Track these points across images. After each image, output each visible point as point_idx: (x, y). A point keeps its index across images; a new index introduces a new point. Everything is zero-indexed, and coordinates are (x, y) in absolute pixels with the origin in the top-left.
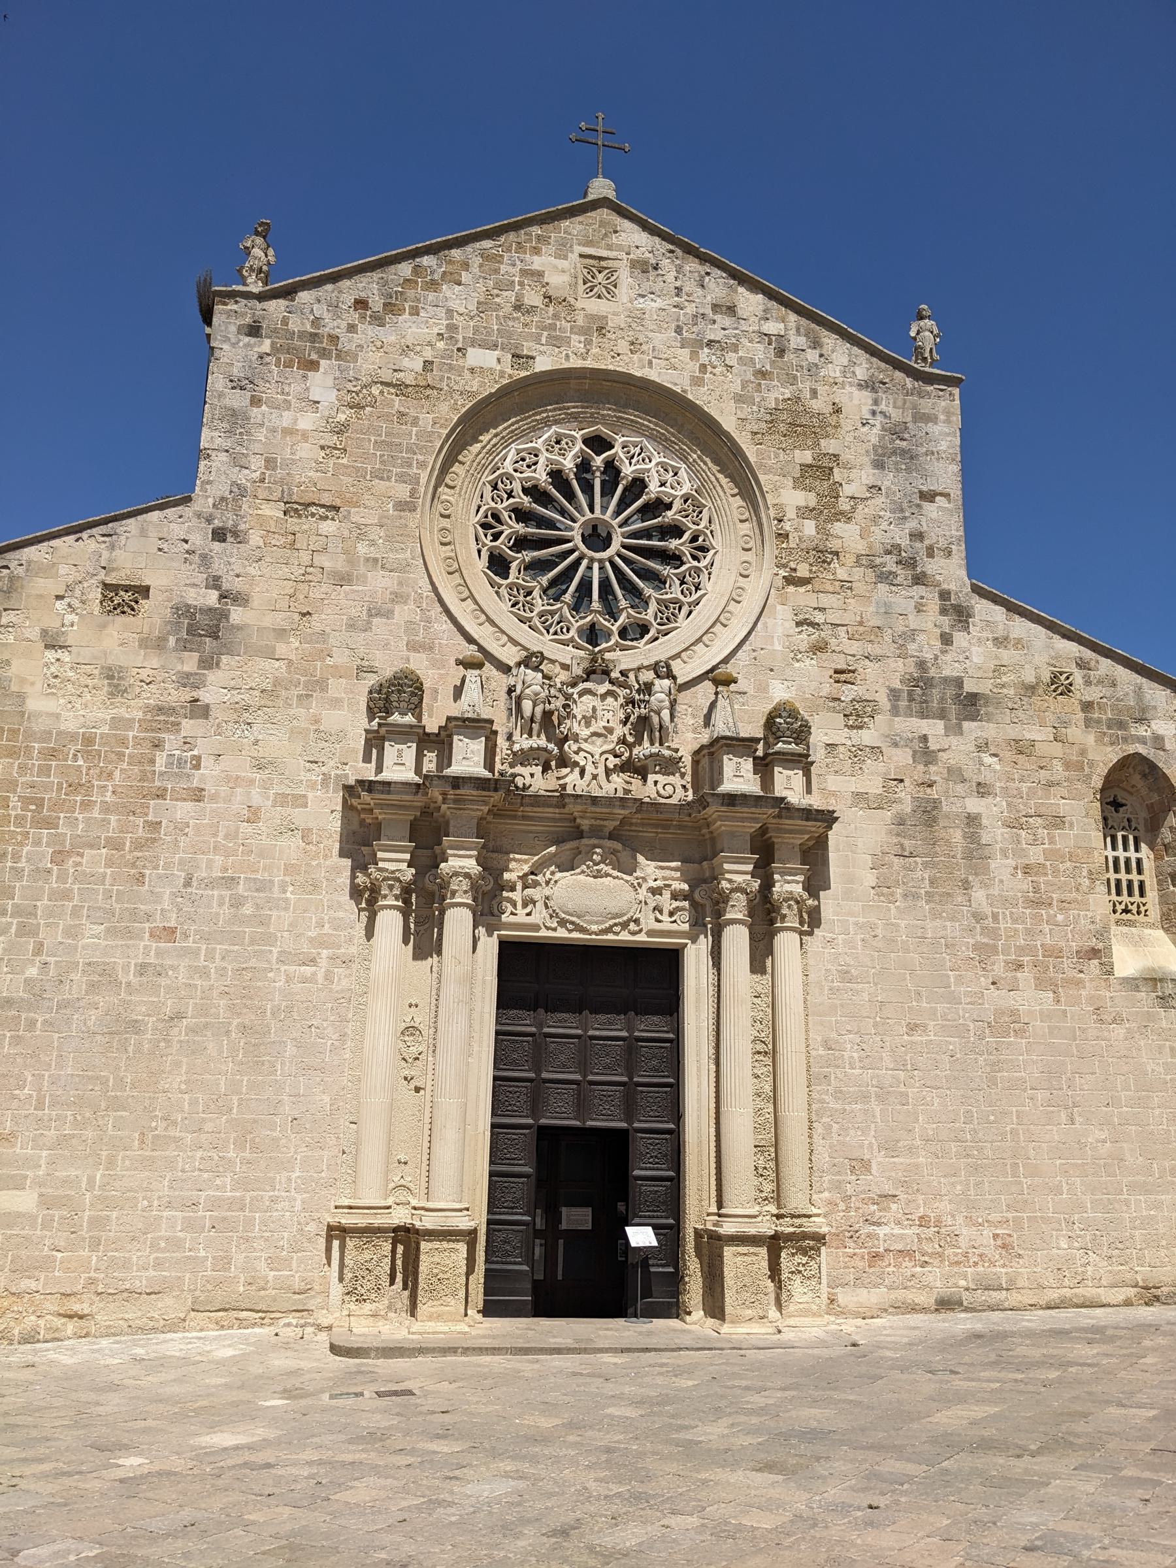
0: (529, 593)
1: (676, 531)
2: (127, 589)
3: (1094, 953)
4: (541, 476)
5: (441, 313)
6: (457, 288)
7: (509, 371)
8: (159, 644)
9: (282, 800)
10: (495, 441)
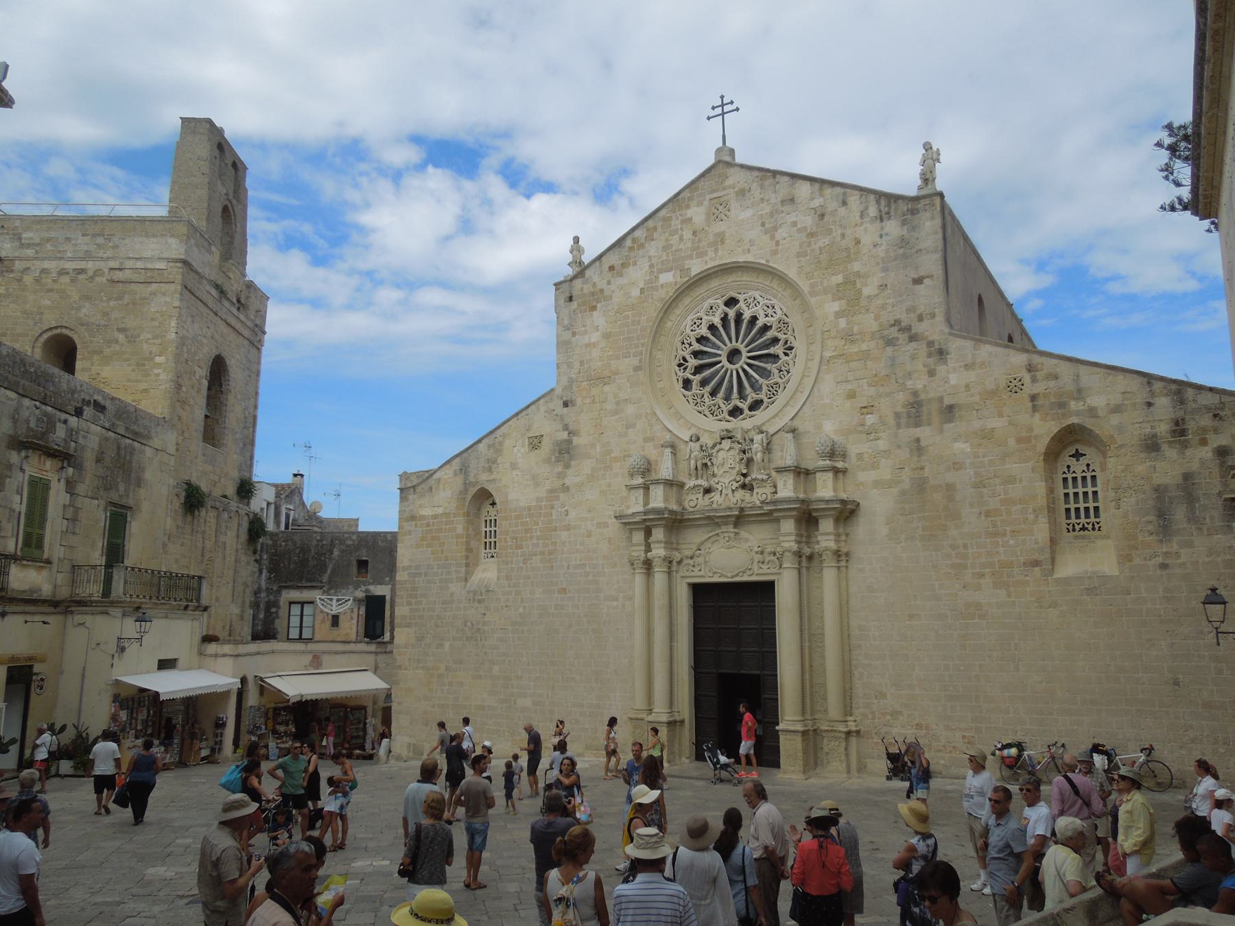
0: (703, 396)
1: (775, 341)
2: (536, 437)
3: (1036, 563)
4: (704, 331)
5: (646, 259)
6: (653, 242)
7: (679, 280)
8: (548, 461)
9: (599, 525)
10: (679, 318)
